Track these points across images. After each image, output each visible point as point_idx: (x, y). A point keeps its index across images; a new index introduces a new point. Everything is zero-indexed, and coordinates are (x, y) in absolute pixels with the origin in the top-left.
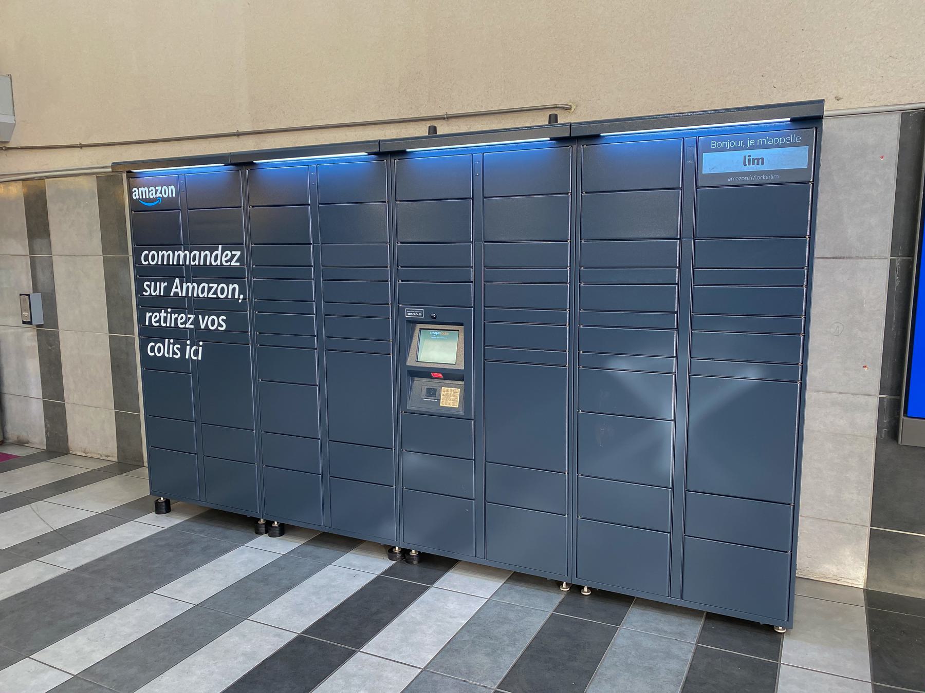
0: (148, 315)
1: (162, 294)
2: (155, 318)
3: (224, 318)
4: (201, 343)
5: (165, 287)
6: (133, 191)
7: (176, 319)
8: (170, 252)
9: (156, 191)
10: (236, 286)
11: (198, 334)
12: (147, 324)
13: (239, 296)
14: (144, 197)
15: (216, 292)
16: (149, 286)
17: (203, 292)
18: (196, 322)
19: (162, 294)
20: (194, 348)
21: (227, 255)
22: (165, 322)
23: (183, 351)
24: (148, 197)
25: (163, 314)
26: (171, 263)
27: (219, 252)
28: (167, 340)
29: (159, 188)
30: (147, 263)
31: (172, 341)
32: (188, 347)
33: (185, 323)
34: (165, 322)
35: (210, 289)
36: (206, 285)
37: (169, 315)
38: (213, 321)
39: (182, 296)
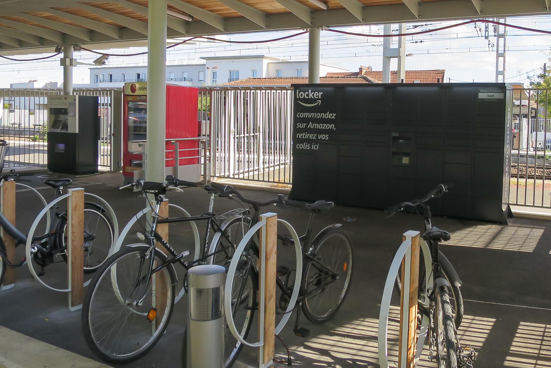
0: (298, 134)
1: (304, 127)
2: (300, 136)
3: (328, 135)
4: (318, 144)
5: (306, 125)
7: (309, 136)
8: (309, 114)
10: (333, 125)
11: (316, 141)
12: (297, 137)
13: (334, 128)
15: (325, 127)
16: (299, 125)
17: (320, 127)
18: (317, 137)
19: (304, 127)
20: (315, 145)
21: (331, 115)
22: (305, 136)
23: (311, 146)
25: (304, 134)
26: (309, 117)
27: (328, 114)
28: (305, 143)
30: (299, 117)
31: (307, 143)
32: (313, 145)
33: (313, 137)
34: (305, 136)
35: (323, 126)
36: (322, 125)
37: (306, 134)
38: (323, 137)
39: (312, 128)
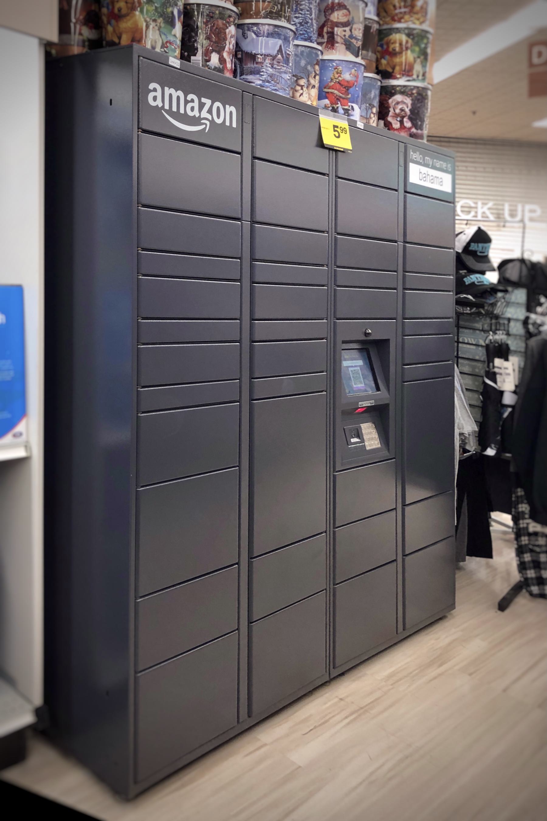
6: (152, 86)
9: (201, 106)
14: (174, 109)
24: (182, 111)
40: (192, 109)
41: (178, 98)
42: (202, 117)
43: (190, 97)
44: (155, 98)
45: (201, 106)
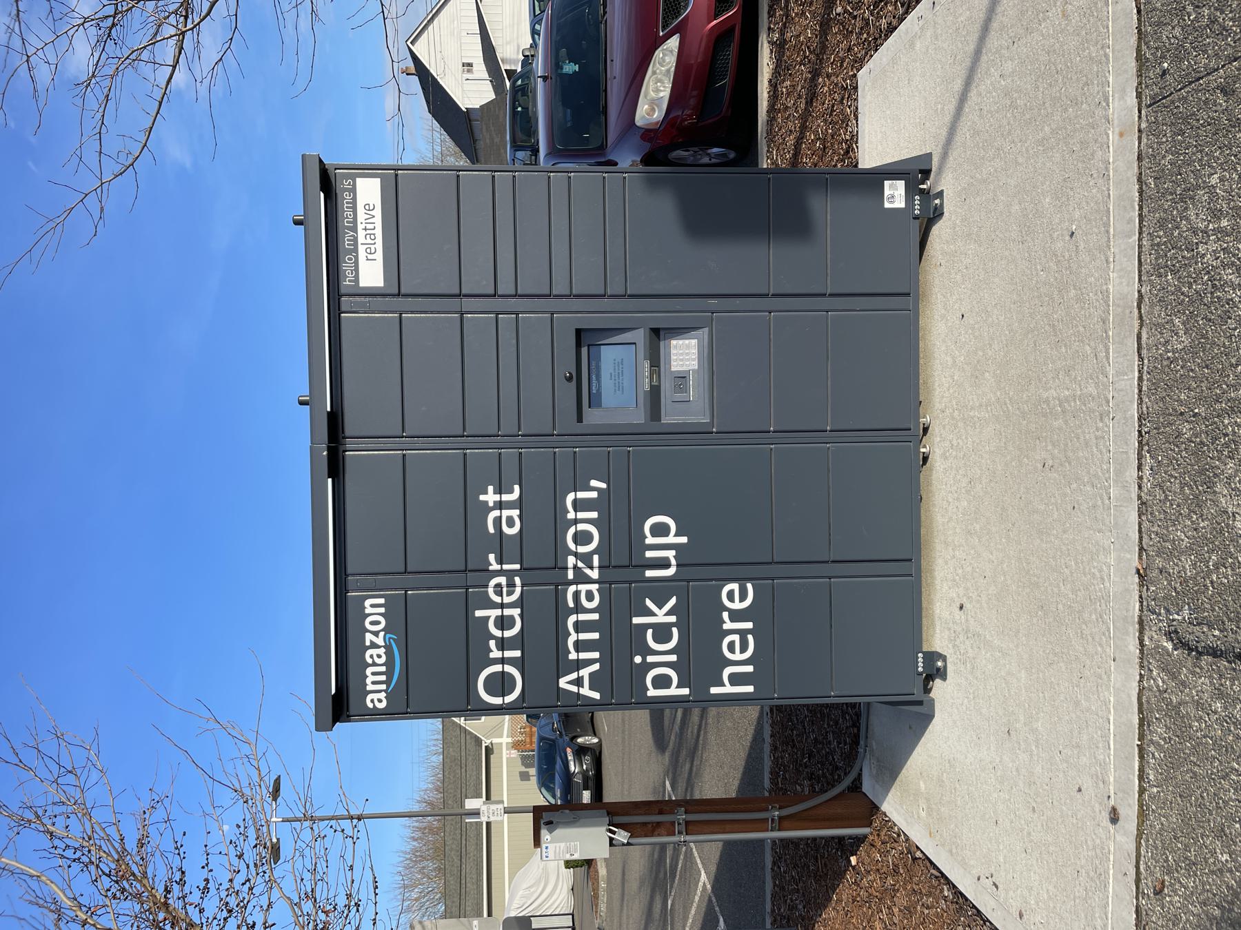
6: (370, 705)
9: (374, 646)
14: (383, 678)
24: (383, 669)
29: (369, 637)
40: (379, 656)
41: (374, 674)
42: (383, 644)
43: (369, 661)
44: (380, 701)
45: (374, 646)
